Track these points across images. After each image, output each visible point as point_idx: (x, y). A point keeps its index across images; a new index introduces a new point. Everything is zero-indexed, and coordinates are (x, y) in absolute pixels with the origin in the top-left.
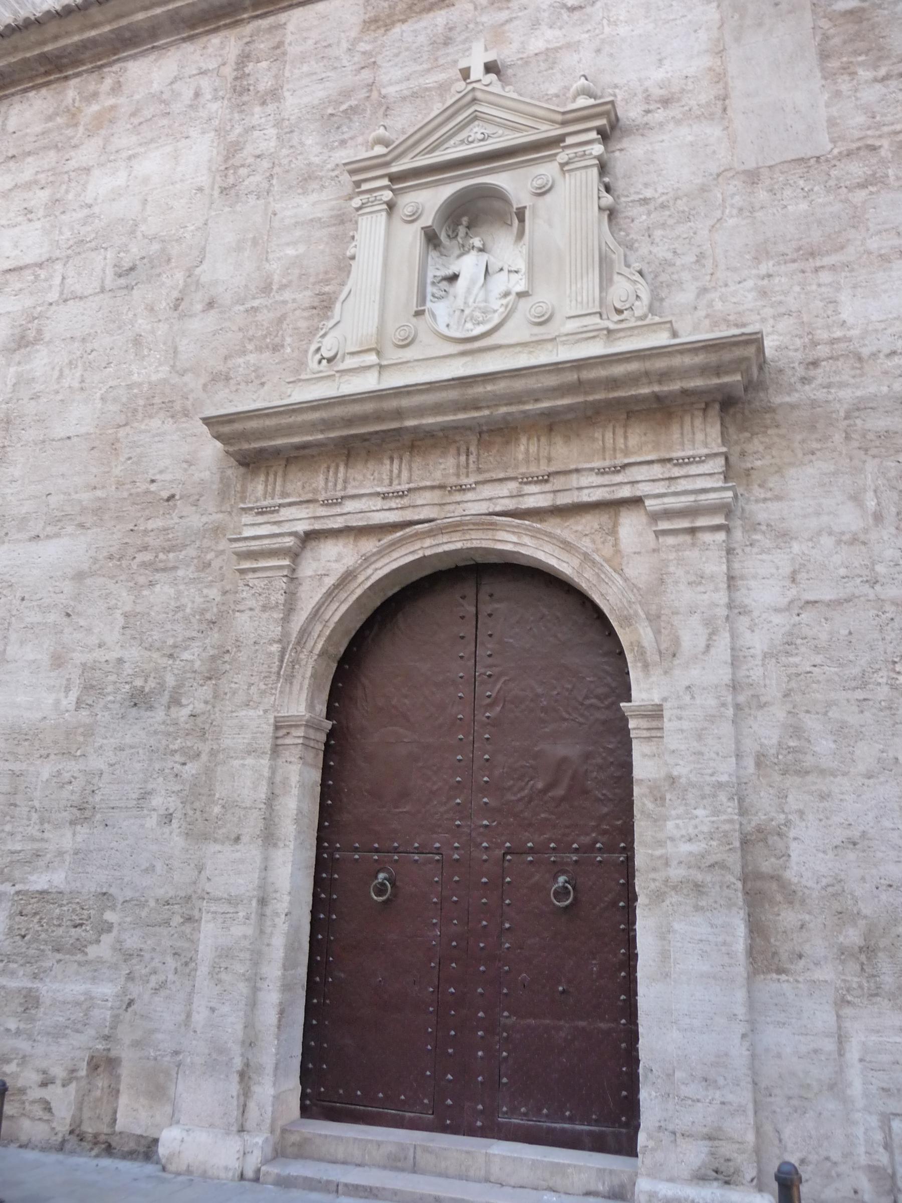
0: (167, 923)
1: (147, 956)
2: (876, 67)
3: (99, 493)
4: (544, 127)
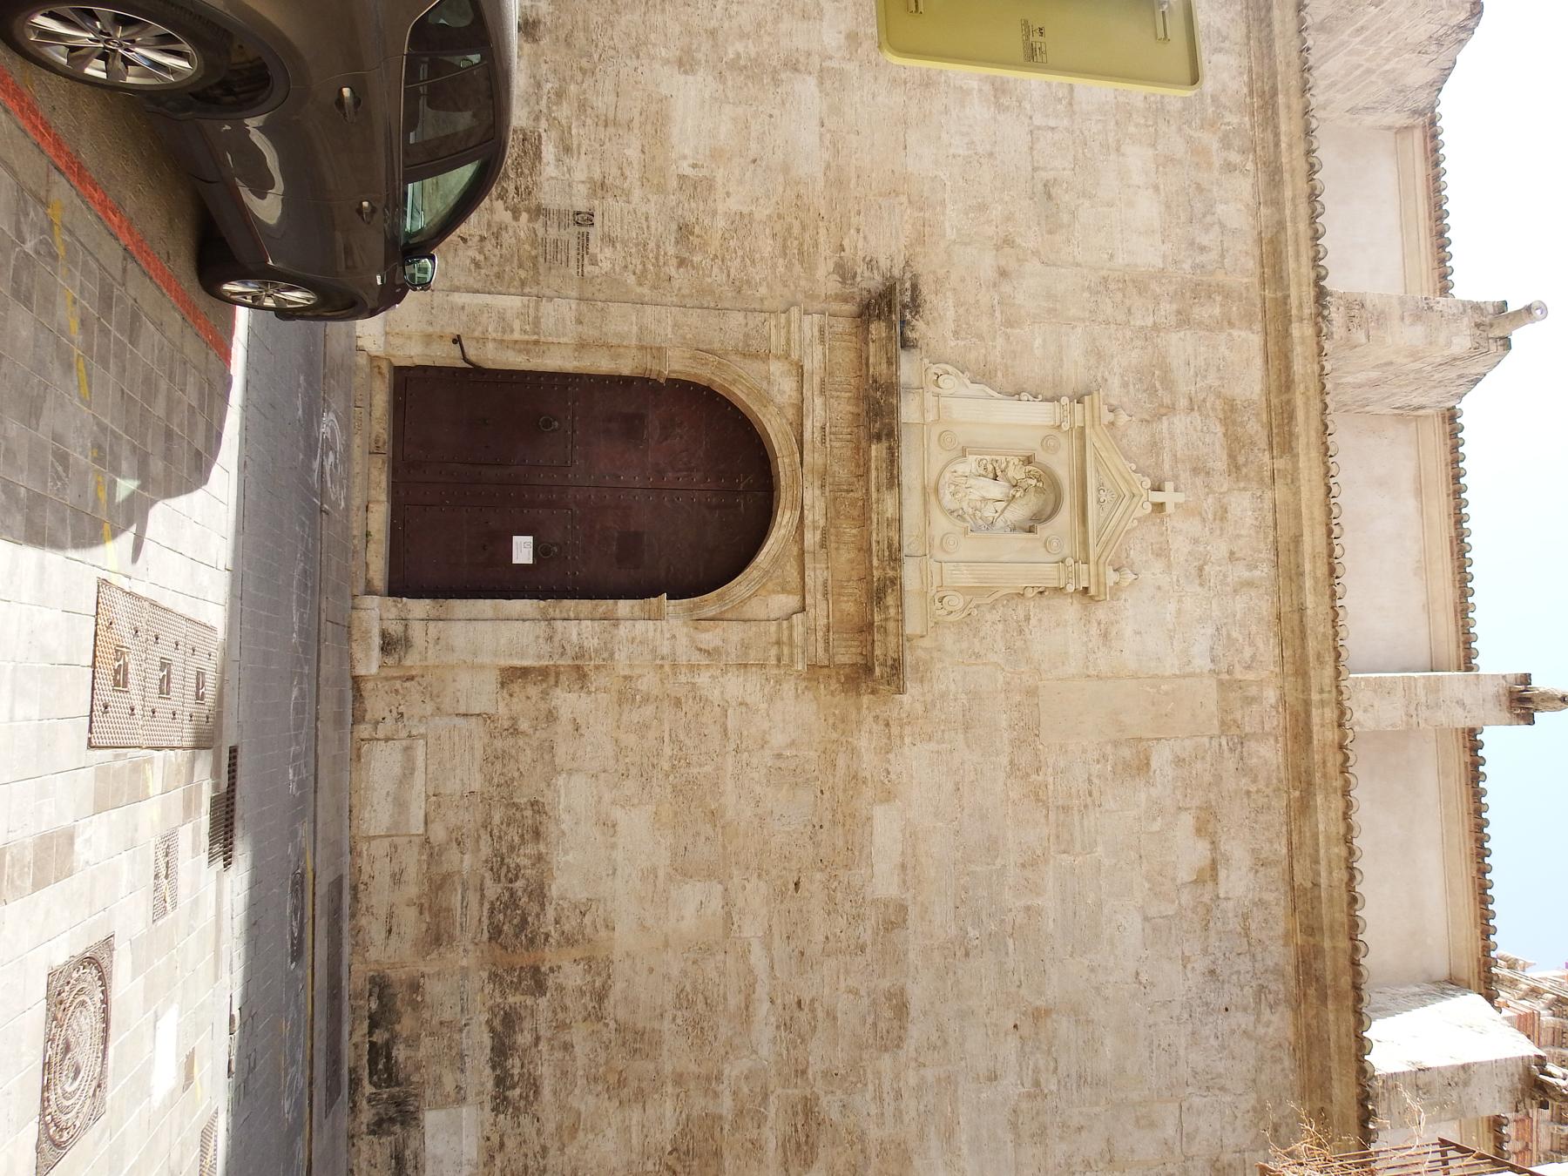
0: (520, 266)
1: (497, 252)
2: (1099, 777)
3: (853, 181)
4: (1098, 549)
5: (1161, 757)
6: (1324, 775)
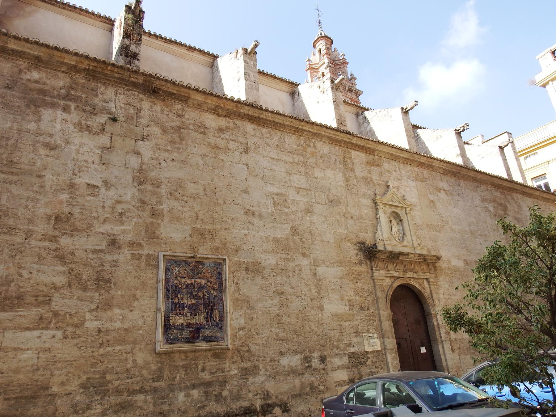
5: (432, 197)
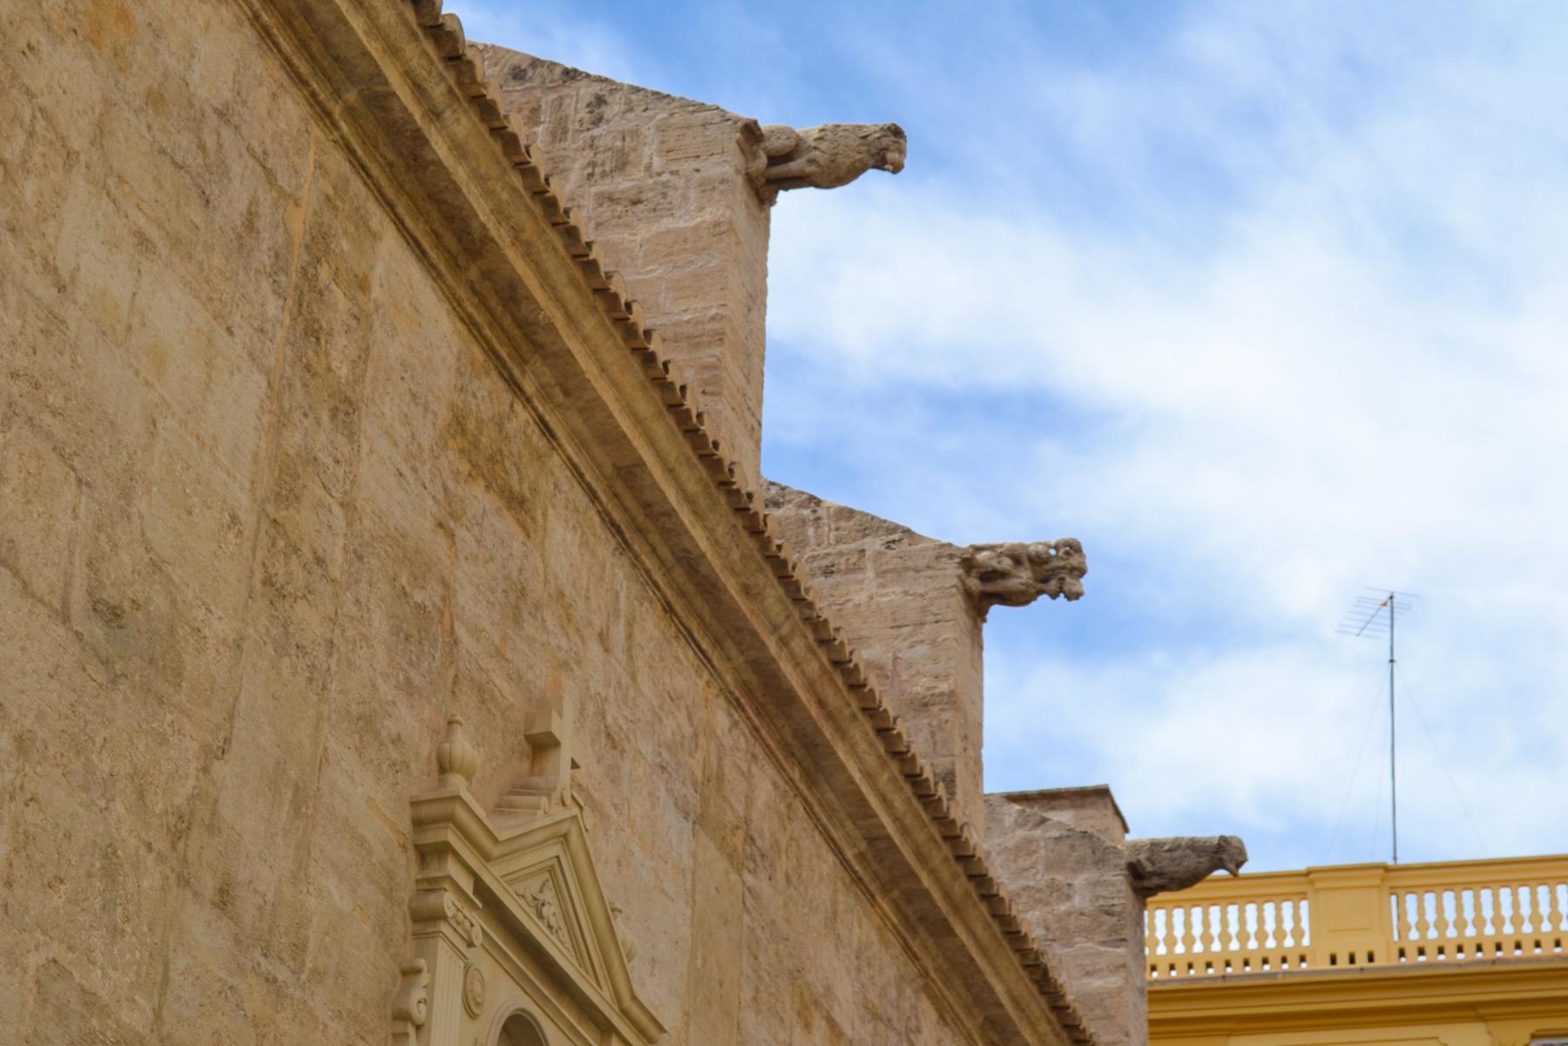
6: (830, 716)
